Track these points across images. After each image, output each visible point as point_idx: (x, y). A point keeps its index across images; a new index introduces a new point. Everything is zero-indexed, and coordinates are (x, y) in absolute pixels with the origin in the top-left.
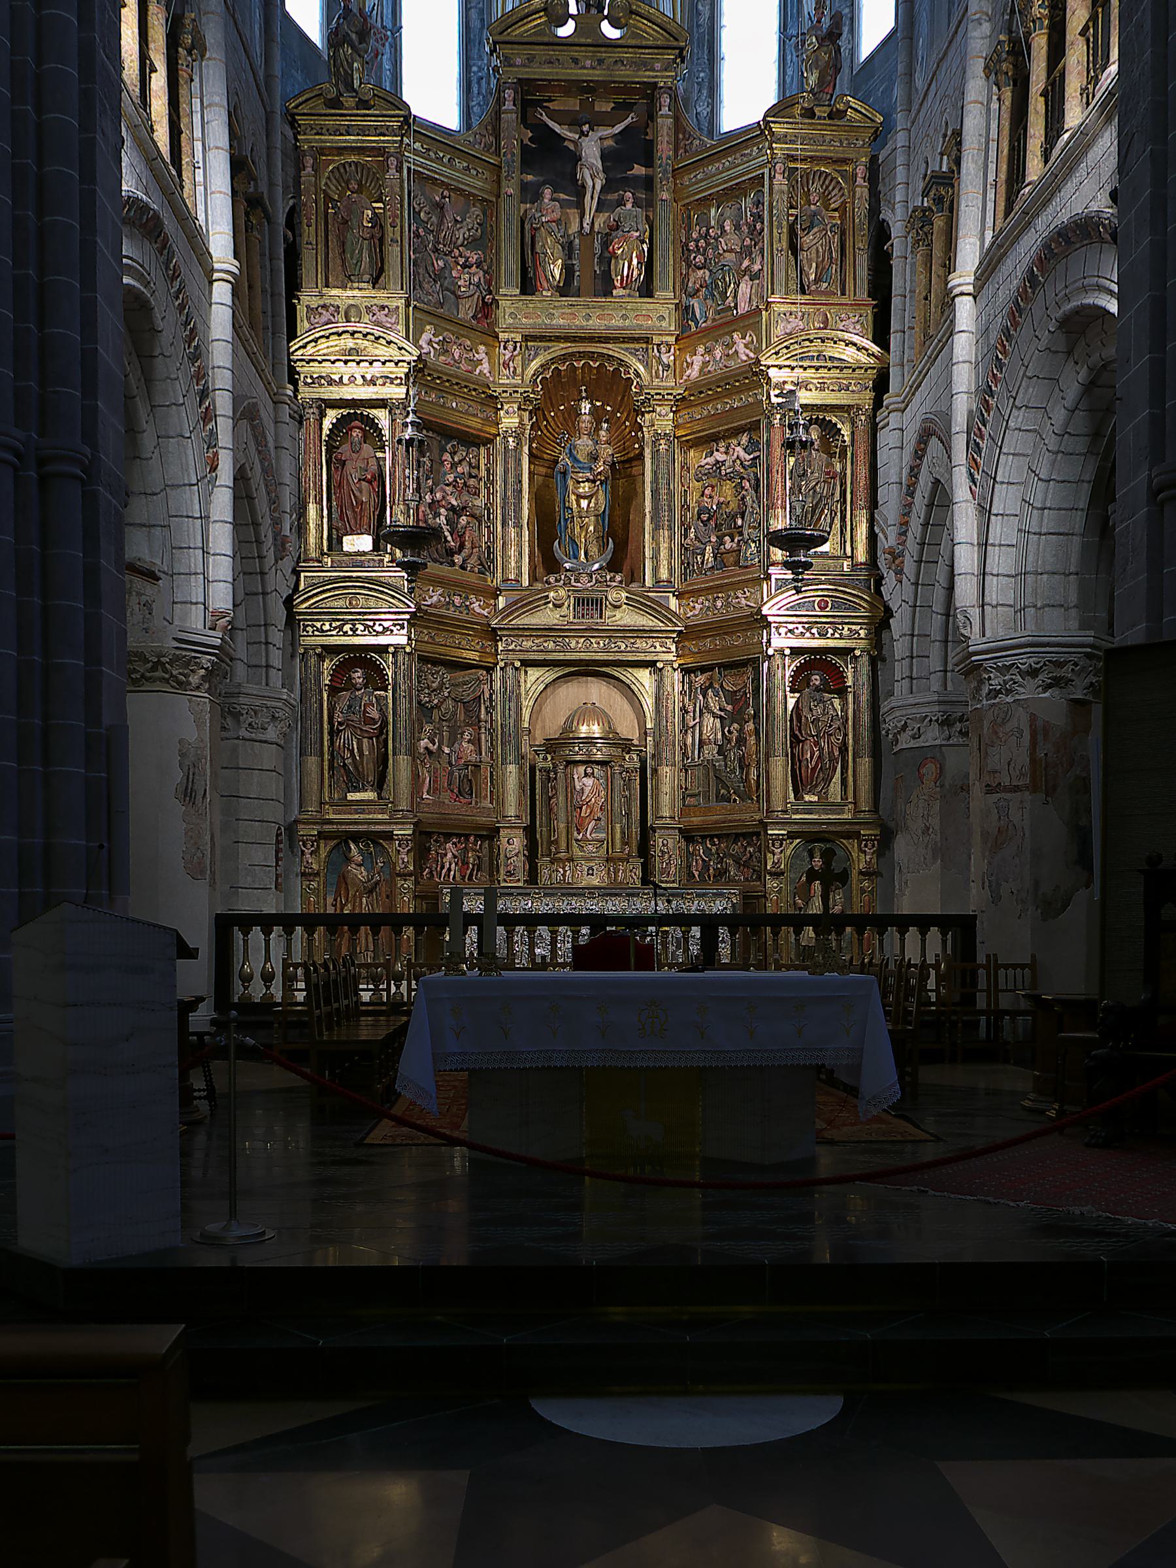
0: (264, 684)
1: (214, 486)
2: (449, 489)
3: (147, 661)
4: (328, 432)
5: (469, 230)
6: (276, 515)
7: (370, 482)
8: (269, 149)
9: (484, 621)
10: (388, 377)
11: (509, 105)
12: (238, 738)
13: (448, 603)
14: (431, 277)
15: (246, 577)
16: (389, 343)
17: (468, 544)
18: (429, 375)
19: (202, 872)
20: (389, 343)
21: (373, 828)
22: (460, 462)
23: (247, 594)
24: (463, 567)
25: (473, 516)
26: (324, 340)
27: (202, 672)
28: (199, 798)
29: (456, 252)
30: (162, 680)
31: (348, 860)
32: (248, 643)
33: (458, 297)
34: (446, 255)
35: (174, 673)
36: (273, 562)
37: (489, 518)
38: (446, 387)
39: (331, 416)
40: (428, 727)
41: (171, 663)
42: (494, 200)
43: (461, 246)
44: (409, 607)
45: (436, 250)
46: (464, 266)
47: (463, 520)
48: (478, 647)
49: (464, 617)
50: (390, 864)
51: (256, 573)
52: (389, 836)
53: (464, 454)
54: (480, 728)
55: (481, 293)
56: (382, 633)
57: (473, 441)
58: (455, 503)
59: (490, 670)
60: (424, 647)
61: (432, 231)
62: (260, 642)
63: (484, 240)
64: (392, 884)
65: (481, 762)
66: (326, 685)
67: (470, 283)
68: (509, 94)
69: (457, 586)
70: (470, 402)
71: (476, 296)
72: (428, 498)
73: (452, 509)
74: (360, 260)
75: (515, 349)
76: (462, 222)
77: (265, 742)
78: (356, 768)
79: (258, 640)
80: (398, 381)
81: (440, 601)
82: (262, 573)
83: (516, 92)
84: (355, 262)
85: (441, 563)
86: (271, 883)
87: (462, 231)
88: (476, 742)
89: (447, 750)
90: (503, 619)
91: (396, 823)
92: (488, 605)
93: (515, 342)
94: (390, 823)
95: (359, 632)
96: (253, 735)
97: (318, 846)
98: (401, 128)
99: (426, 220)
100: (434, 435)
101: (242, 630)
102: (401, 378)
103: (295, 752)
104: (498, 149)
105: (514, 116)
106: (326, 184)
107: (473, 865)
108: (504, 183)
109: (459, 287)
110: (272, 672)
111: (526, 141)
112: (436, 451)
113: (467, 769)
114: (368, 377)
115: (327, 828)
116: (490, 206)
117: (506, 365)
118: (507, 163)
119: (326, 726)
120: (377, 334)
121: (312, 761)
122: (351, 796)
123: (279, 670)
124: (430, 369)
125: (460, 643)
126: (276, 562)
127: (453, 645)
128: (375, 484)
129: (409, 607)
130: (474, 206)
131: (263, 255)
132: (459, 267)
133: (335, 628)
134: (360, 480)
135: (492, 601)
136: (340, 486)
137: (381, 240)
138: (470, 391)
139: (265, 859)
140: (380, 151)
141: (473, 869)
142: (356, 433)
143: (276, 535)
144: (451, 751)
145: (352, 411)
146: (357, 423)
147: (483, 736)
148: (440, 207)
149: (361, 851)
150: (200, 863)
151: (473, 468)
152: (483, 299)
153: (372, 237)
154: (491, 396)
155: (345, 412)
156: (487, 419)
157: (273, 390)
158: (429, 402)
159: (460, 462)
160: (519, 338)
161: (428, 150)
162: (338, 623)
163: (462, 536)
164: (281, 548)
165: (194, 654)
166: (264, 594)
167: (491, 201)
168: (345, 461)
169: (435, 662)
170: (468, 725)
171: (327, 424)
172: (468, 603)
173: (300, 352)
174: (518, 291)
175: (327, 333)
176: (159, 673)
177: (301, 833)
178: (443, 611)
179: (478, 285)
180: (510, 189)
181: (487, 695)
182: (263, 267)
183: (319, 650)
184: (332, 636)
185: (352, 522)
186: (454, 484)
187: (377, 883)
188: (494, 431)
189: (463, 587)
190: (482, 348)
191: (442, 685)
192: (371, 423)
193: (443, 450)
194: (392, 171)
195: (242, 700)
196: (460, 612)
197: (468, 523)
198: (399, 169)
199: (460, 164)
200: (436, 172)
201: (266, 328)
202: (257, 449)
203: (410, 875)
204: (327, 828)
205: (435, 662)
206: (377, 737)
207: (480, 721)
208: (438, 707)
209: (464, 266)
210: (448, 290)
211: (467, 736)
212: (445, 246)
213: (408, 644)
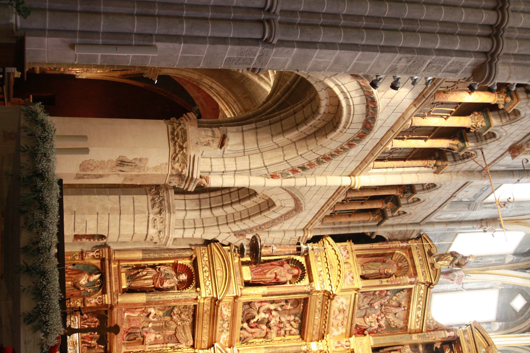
0: (176, 227)
1: (265, 177)
2: (278, 320)
3: (183, 143)
4: (294, 258)
5: (393, 321)
6: (255, 230)
7: (275, 278)
8: (406, 224)
9: (217, 340)
10: (323, 281)
11: (448, 334)
12: (149, 214)
13: (223, 320)
14: (370, 301)
15: (225, 217)
16: (339, 281)
17: (253, 330)
18: (328, 302)
19: (83, 170)
20: (339, 281)
21: (108, 284)
22: (291, 325)
23: (217, 218)
24: (242, 329)
25: (267, 333)
26: (334, 252)
27: (180, 170)
28: (120, 168)
29: (383, 315)
30: (175, 150)
31: (90, 274)
32: (194, 220)
33: (364, 317)
34: (381, 310)
35: (179, 155)
36: (234, 230)
37: (267, 341)
38: (324, 312)
39: (302, 259)
40: (161, 313)
41: (184, 154)
42: (408, 331)
43: (386, 318)
44: (220, 296)
45: (381, 305)
46: (378, 320)
47: (264, 327)
48: (204, 338)
49: (218, 330)
50: (90, 295)
51: (227, 221)
52: (104, 292)
53: (295, 327)
54: (163, 344)
55: (368, 328)
56: (205, 285)
57: (302, 330)
58: (272, 322)
59: (193, 347)
60: (201, 308)
61: (389, 303)
62: (195, 225)
63: (391, 329)
64: (79, 296)
65: (146, 345)
66: (177, 261)
67: (371, 322)
68: (452, 334)
69: (232, 325)
70: (319, 326)
71: (366, 325)
72: (272, 307)
73: (269, 322)
74: (370, 269)
75: (347, 346)
76: (396, 317)
77: (148, 228)
78: (138, 278)
79: (196, 224)
80: (322, 287)
81: (224, 315)
82: (227, 224)
83: (454, 337)
84: (369, 267)
85: (242, 316)
86: (78, 232)
87: (392, 317)
88: (156, 341)
89: (150, 325)
90: (220, 349)
91: (111, 295)
92: (225, 343)
93: (349, 346)
94: (111, 292)
95: (205, 274)
96: (150, 222)
97: (97, 259)
98: (427, 282)
99: (393, 299)
100: (301, 310)
101: (200, 215)
102: (324, 288)
103: (144, 246)
104: (430, 331)
105: (444, 336)
106: (398, 253)
107: (90, 344)
108: (416, 335)
109: (368, 317)
110: (181, 231)
111: (435, 346)
112: (294, 311)
113: (142, 337)
114: (322, 273)
115: (107, 262)
116: (405, 330)
117: (339, 343)
118: (424, 336)
119: (157, 262)
120: (341, 275)
121: (139, 255)
122: (123, 276)
123: (183, 236)
124: (331, 302)
125: (205, 328)
126: (234, 232)
127: (204, 324)
128: (275, 281)
129: (220, 296)
130: (404, 323)
131: (364, 222)
132: (376, 317)
133: (205, 263)
134: (276, 273)
135: (227, 345)
136: (272, 265)
137: (380, 278)
138: (324, 325)
139: (89, 229)
140: (416, 274)
141: (88, 343)
142: (296, 271)
143: (245, 231)
144: (150, 328)
145: (306, 268)
146: (301, 272)
147: (158, 346)
148: (399, 306)
149: (95, 281)
150: (88, 168)
151: (289, 333)
152: (365, 329)
153: (381, 274)
154: (323, 337)
155: (305, 265)
156: (313, 336)
157: (309, 227)
158: (316, 304)
159: (291, 325)
160: (352, 347)
161: (421, 297)
162: (208, 264)
163: (256, 327)
164: (240, 234)
165: (188, 165)
166: (218, 225)
167: (407, 330)
168: (283, 266)
169: (194, 316)
170: (164, 337)
171: (298, 258)
172: (225, 331)
173: (327, 243)
174: (372, 345)
175: (337, 253)
176: (178, 149)
177: (103, 250)
178: (219, 318)
179: (371, 326)
180: (415, 338)
181: (180, 346)
182: (359, 222)
183: (194, 256)
184: (202, 262)
185: (256, 271)
186: (281, 322)
187: (79, 289)
188: (308, 340)
189: (232, 329)
190: (344, 331)
191: (183, 320)
192: (302, 277)
193: (295, 315)
194: (409, 280)
195: (167, 215)
196: (220, 328)
197: (263, 330)
198: (411, 283)
199: (419, 313)
200: (413, 301)
201: (334, 224)
202: (283, 215)
203: (84, 305)
204: (107, 262)
205: (194, 316)
206: (154, 287)
207: (166, 343)
208: (172, 319)
209: (378, 320)
210: (366, 312)
211: (158, 336)
212: (384, 309)
213: (202, 298)
